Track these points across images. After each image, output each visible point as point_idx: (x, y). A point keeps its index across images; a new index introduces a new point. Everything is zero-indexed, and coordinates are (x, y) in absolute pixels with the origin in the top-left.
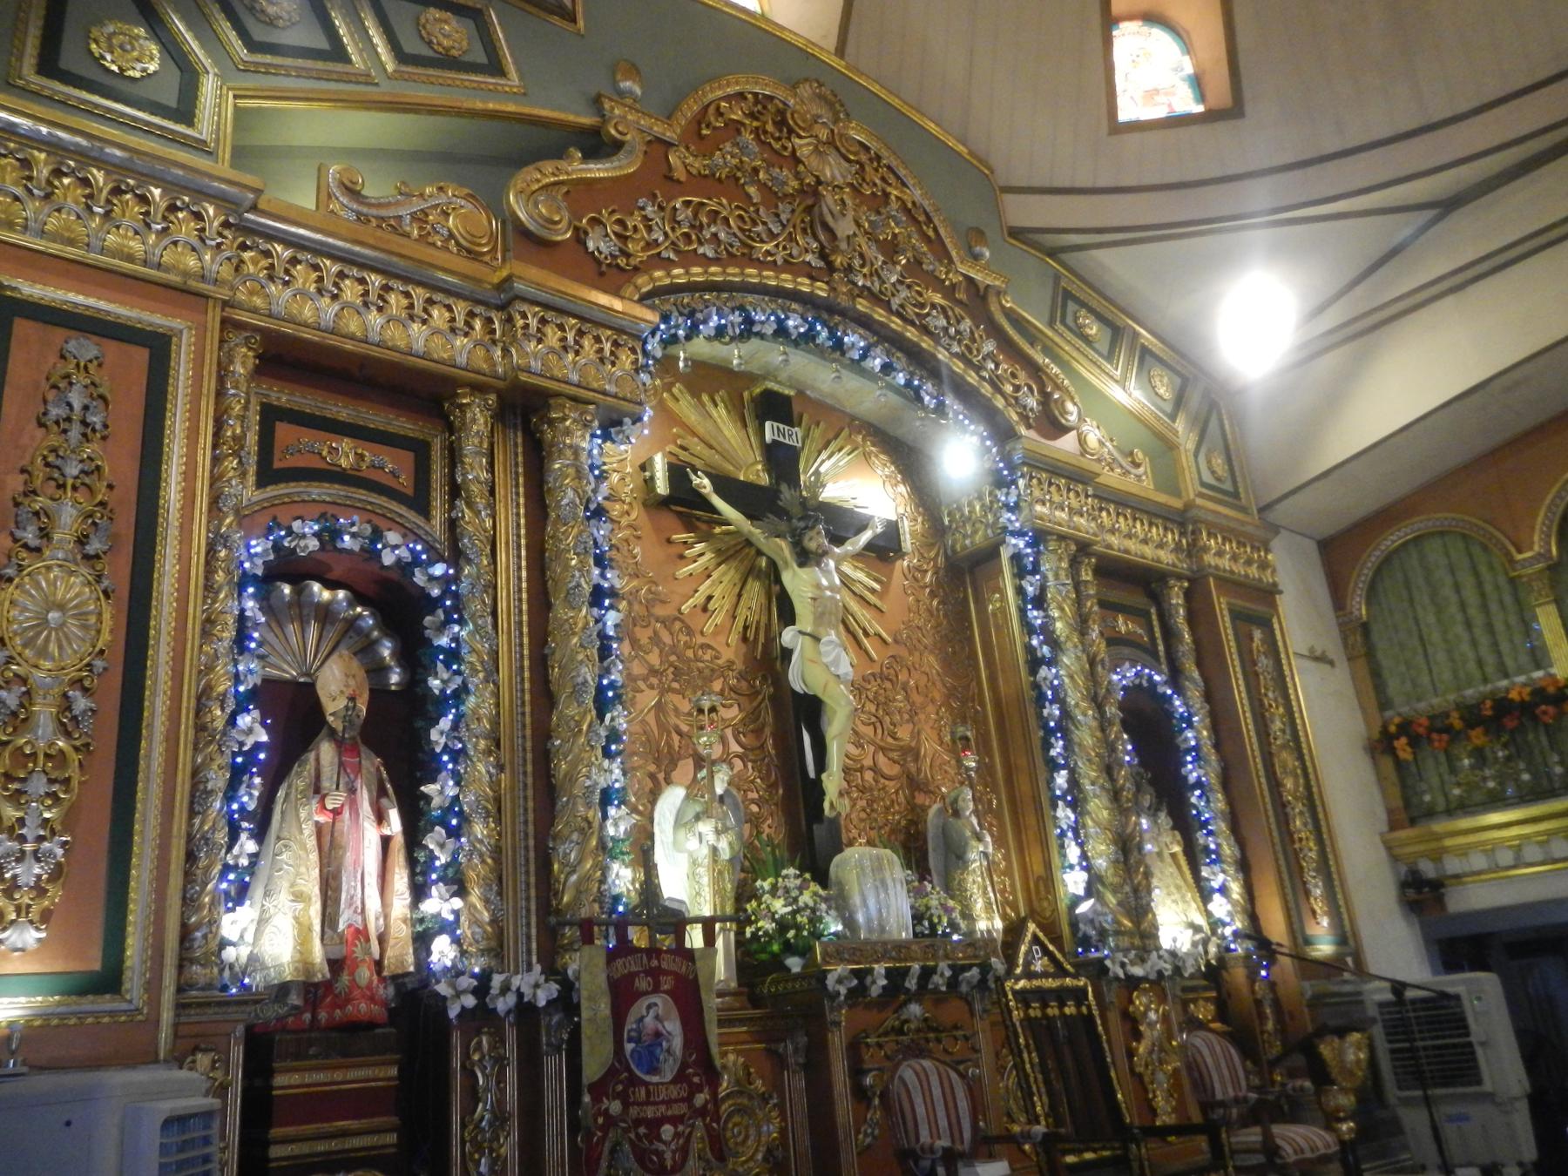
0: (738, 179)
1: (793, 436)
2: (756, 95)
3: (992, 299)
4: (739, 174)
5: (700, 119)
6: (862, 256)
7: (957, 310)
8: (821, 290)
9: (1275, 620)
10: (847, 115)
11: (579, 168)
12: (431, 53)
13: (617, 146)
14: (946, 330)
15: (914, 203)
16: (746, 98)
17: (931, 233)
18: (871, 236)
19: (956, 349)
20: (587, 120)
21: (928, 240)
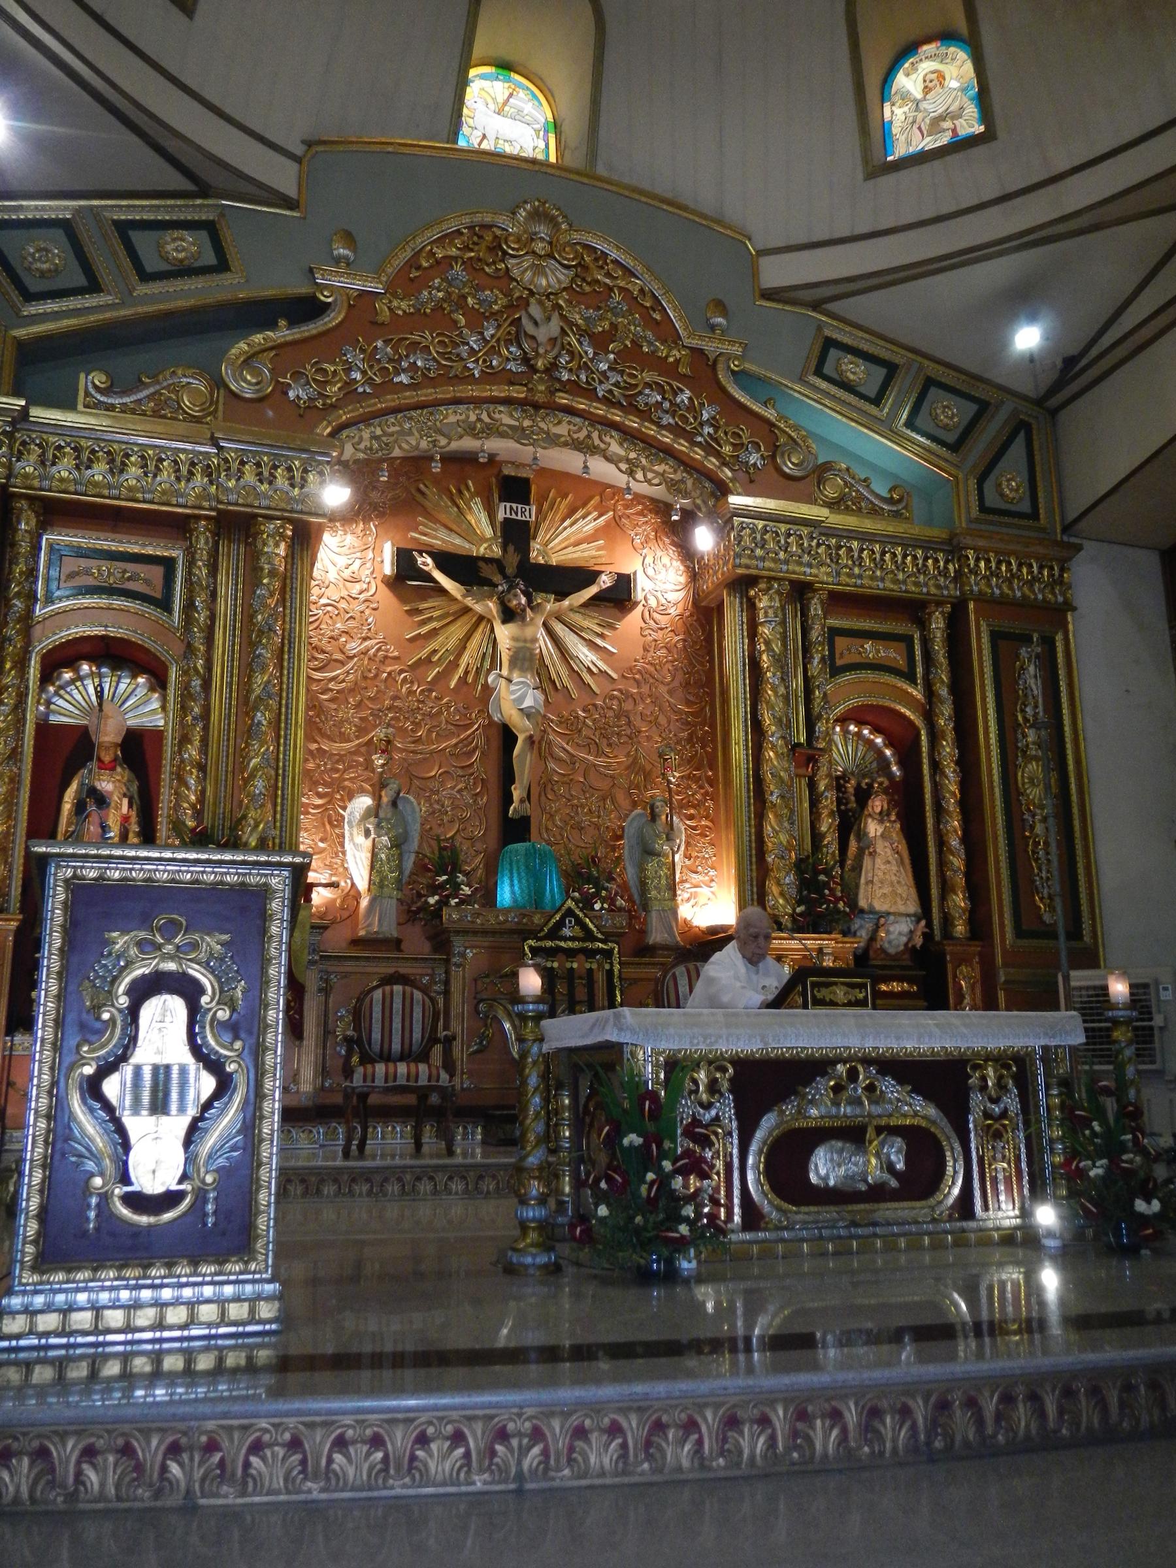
0: (444, 309)
1: (528, 513)
2: (471, 228)
3: (720, 366)
4: (445, 305)
5: (413, 263)
6: (571, 353)
7: (675, 384)
8: (519, 393)
9: (1059, 637)
10: (570, 225)
11: (283, 333)
12: (169, 268)
13: (324, 308)
14: (659, 404)
15: (642, 291)
16: (462, 234)
17: (657, 316)
18: (582, 333)
19: (667, 420)
20: (304, 290)
21: (649, 322)
